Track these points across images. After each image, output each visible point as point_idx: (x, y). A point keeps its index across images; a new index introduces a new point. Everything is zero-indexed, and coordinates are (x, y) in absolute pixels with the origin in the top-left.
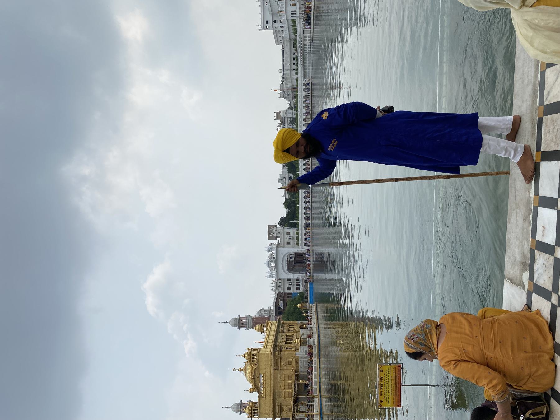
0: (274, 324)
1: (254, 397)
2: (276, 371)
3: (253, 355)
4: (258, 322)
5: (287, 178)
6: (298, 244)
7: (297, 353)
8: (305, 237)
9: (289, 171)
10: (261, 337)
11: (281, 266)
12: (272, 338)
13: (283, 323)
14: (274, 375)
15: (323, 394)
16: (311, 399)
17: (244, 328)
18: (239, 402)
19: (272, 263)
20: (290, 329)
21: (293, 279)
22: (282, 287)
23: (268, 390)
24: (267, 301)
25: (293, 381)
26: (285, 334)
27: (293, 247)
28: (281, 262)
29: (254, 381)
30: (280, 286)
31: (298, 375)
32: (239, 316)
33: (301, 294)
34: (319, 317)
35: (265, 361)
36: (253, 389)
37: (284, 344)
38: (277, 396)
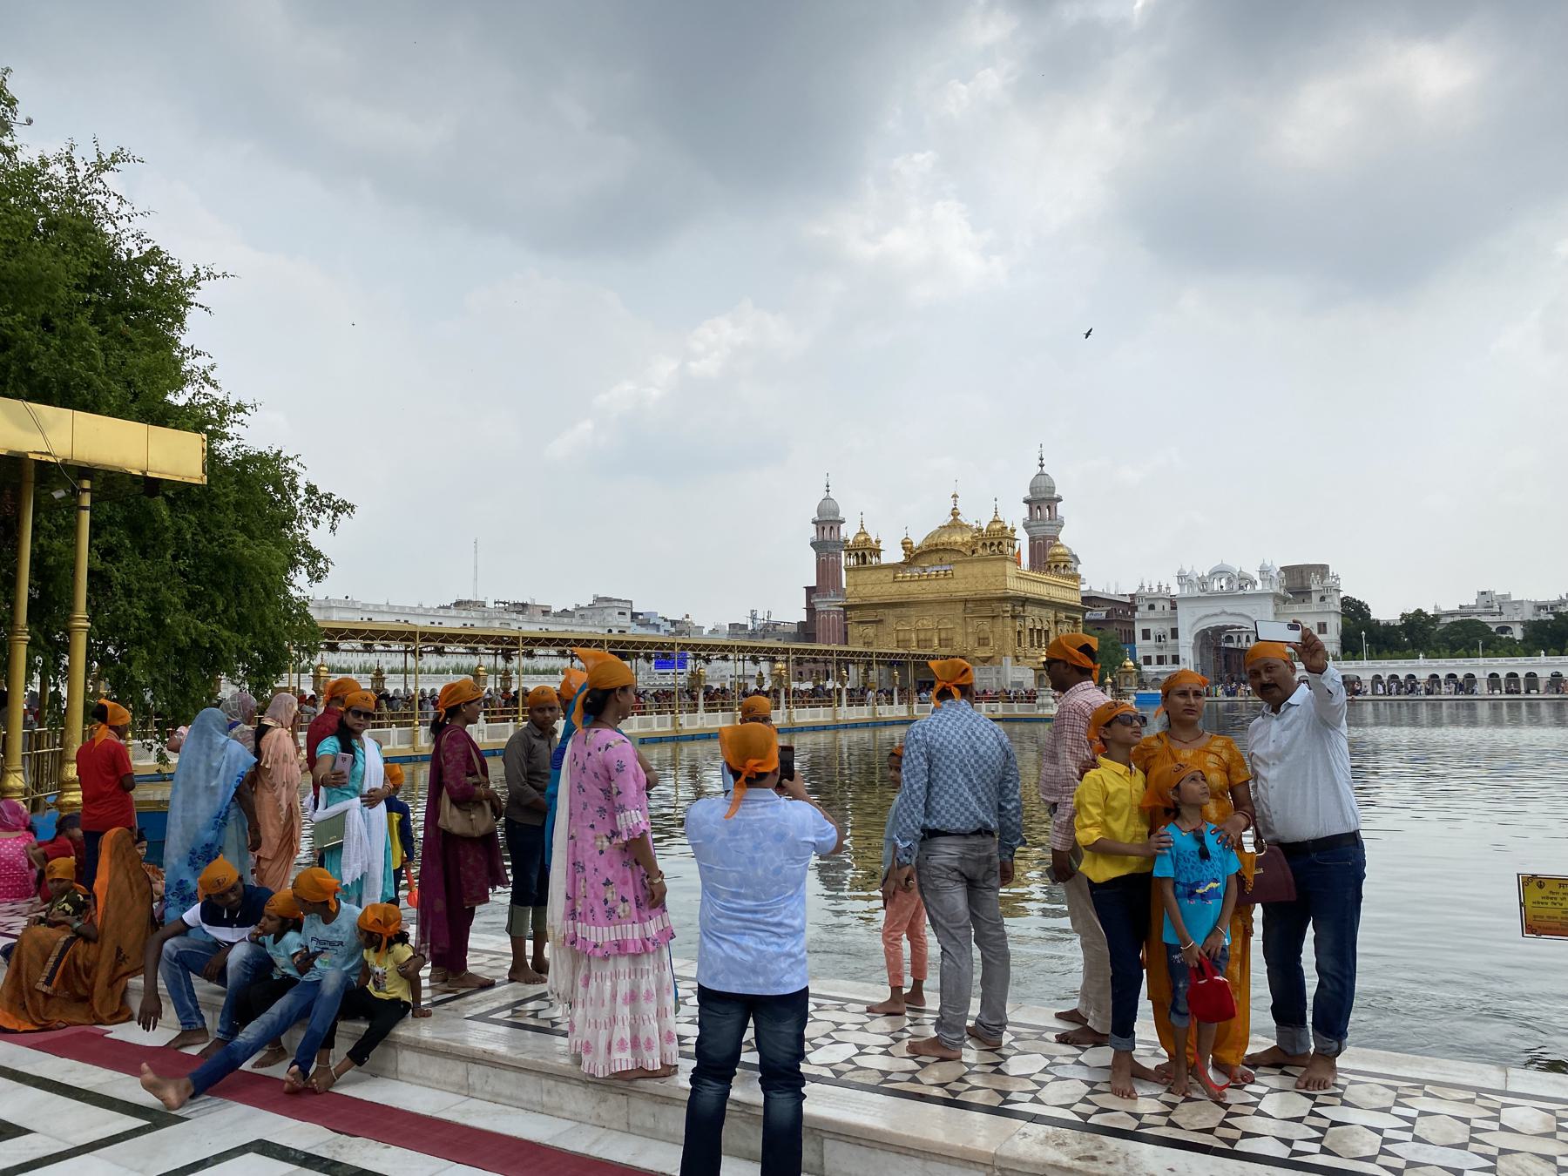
0: (1075, 598)
2: (961, 607)
4: (1048, 556)
11: (1217, 611)
13: (1076, 621)
16: (905, 697)
17: (1026, 514)
18: (841, 515)
19: (1223, 582)
21: (1177, 647)
22: (1152, 614)
23: (914, 589)
28: (1229, 610)
30: (1152, 607)
32: (1059, 500)
35: (985, 576)
36: (911, 550)
37: (1029, 624)
38: (898, 611)
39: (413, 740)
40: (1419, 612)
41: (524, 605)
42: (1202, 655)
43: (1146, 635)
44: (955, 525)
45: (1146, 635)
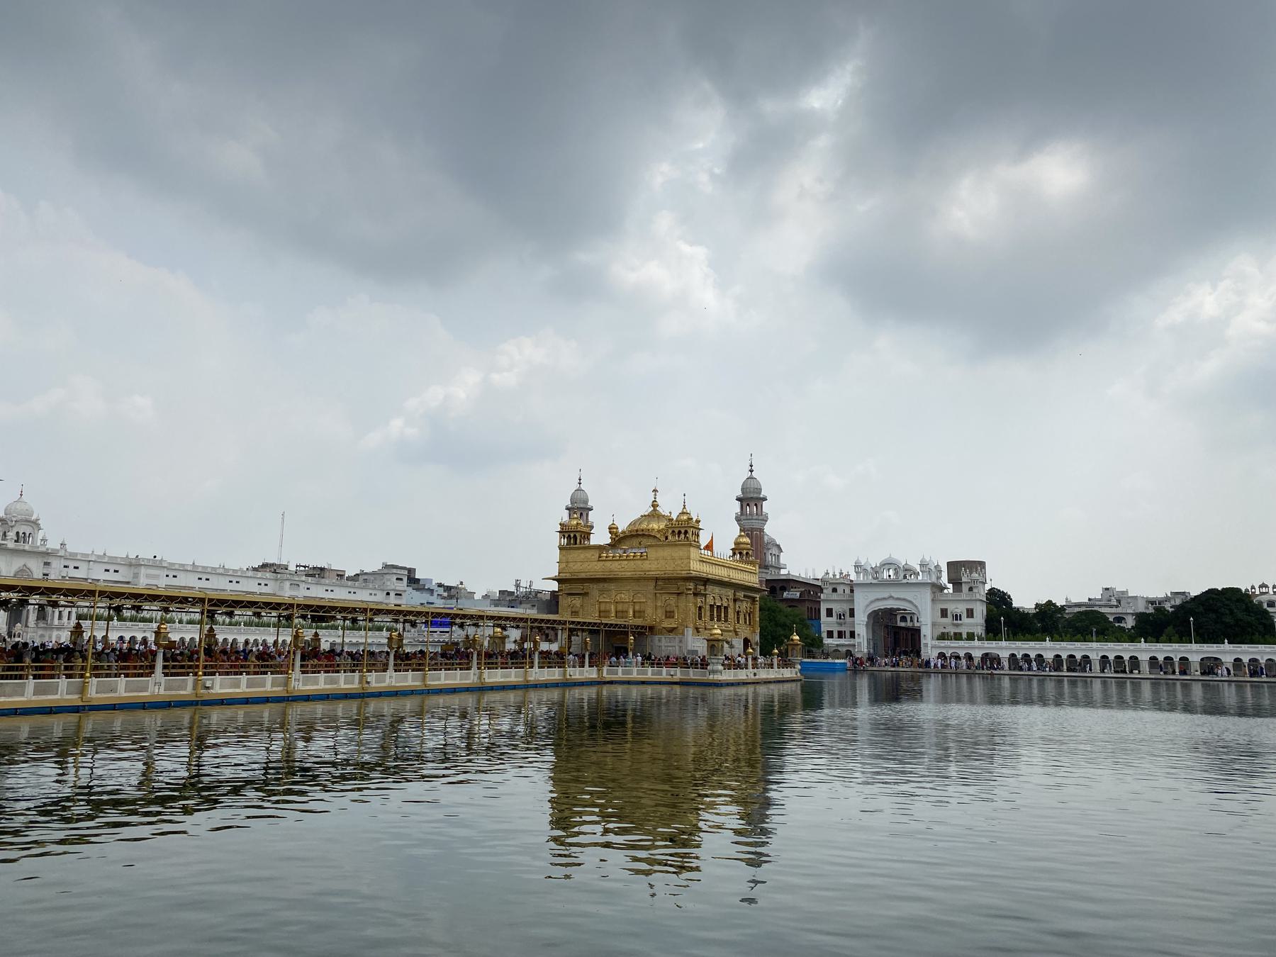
0: (752, 578)
1: (600, 537)
3: (686, 532)
4: (754, 544)
5: (1119, 610)
6: (943, 637)
7: (690, 632)
8: (962, 654)
9: (1141, 617)
10: (724, 549)
11: (886, 595)
12: (721, 573)
13: (753, 599)
14: (645, 579)
15: (605, 690)
17: (738, 510)
19: (891, 572)
20: (742, 616)
21: (853, 624)
22: (835, 596)
23: (616, 568)
24: (801, 561)
25: (632, 621)
26: (731, 604)
27: (934, 625)
29: (632, 536)
30: (835, 590)
31: (645, 632)
32: (765, 499)
33: (818, 642)
34: (772, 686)
35: (673, 559)
36: (616, 534)
37: (710, 601)
38: (601, 585)
39: (82, 690)
40: (1050, 602)
41: (322, 569)
42: (874, 632)
43: (830, 613)
44: (655, 514)
45: (830, 613)
